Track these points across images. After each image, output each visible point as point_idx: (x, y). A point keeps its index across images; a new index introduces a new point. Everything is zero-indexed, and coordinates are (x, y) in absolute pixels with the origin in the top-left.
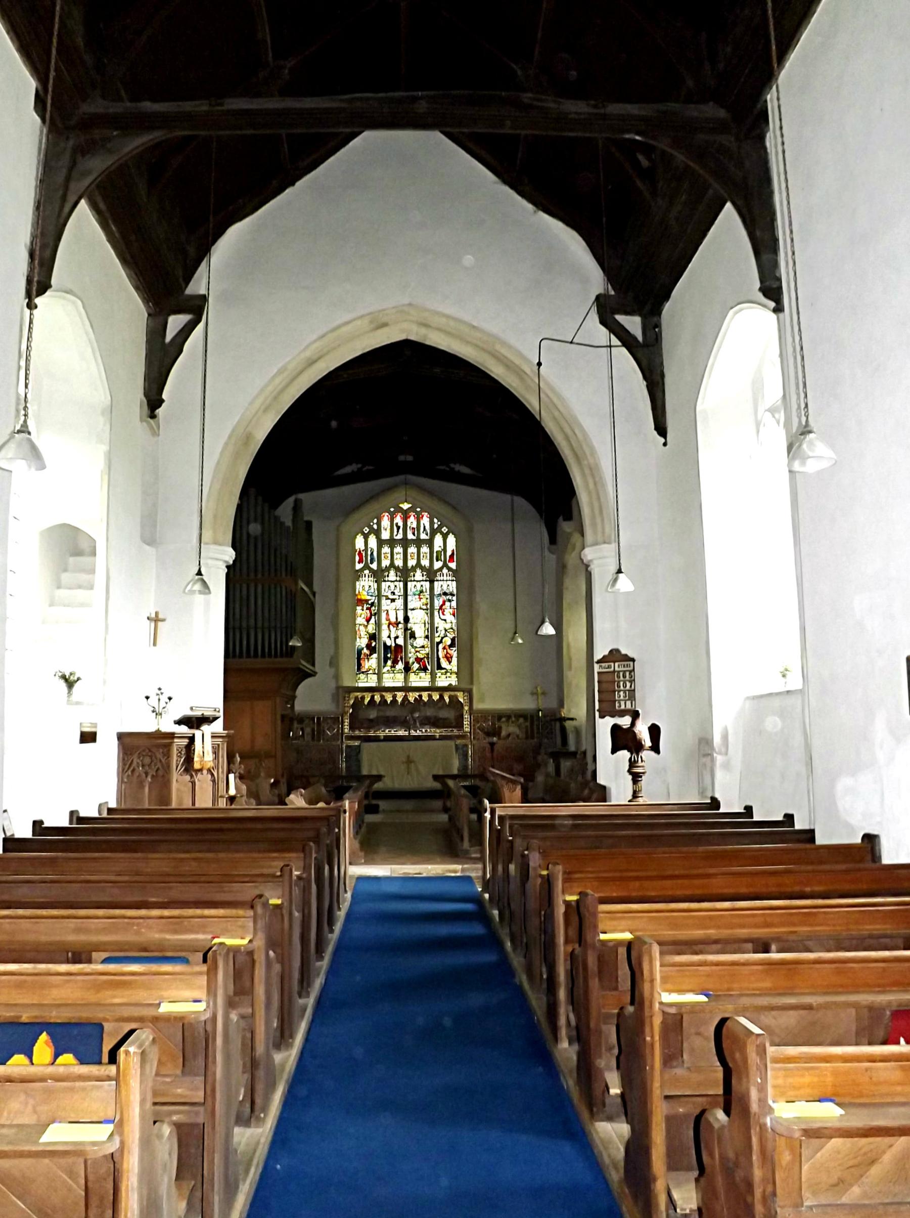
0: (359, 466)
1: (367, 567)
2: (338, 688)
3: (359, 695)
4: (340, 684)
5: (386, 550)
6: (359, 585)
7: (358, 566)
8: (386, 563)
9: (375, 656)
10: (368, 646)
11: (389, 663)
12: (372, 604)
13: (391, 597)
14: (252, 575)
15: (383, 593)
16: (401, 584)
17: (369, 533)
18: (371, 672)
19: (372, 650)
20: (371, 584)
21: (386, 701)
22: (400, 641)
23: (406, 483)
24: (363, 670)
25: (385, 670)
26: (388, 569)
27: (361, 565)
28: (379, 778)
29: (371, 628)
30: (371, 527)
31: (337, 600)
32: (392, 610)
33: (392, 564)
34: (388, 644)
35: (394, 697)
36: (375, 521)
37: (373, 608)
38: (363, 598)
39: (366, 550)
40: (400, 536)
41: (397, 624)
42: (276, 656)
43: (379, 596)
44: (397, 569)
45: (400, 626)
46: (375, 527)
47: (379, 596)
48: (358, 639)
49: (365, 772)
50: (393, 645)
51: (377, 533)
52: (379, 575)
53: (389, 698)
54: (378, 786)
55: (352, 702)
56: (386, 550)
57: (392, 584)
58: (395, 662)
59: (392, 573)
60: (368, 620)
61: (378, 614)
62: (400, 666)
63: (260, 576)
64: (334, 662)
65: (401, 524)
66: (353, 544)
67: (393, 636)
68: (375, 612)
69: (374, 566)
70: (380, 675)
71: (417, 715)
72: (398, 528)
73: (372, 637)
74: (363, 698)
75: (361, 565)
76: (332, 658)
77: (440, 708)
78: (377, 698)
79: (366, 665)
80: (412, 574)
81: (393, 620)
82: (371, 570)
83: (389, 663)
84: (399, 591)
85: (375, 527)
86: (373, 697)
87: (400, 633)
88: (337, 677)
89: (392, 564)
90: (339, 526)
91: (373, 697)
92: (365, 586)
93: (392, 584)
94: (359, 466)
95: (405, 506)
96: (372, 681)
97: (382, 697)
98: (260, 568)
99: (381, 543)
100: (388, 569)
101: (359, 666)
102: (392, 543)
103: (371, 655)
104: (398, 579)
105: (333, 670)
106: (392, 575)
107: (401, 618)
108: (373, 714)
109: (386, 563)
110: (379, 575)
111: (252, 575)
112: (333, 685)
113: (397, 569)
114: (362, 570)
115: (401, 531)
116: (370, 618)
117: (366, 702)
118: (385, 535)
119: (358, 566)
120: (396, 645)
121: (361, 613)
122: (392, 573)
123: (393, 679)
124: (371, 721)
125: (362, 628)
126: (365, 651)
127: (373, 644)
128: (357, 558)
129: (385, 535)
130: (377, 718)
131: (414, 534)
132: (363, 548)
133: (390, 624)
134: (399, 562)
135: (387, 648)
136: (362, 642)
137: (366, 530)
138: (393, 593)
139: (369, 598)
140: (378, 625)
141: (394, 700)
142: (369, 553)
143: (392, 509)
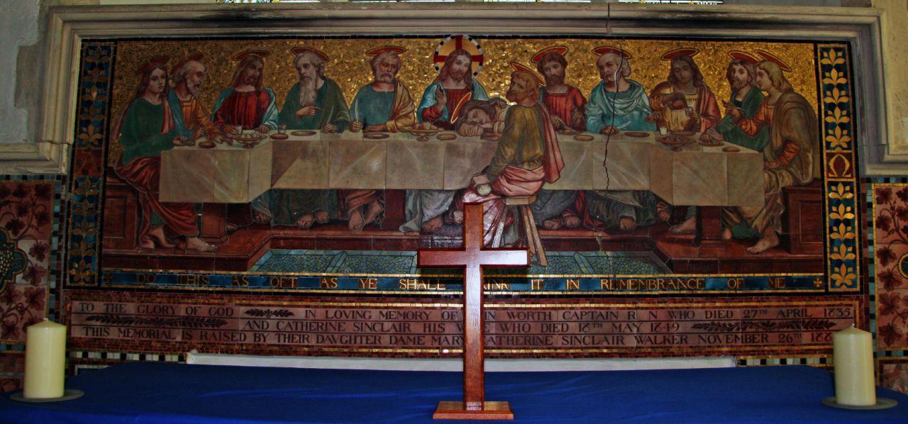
71: (522, 188)
77: (675, 143)
124: (238, 214)
130: (277, 197)
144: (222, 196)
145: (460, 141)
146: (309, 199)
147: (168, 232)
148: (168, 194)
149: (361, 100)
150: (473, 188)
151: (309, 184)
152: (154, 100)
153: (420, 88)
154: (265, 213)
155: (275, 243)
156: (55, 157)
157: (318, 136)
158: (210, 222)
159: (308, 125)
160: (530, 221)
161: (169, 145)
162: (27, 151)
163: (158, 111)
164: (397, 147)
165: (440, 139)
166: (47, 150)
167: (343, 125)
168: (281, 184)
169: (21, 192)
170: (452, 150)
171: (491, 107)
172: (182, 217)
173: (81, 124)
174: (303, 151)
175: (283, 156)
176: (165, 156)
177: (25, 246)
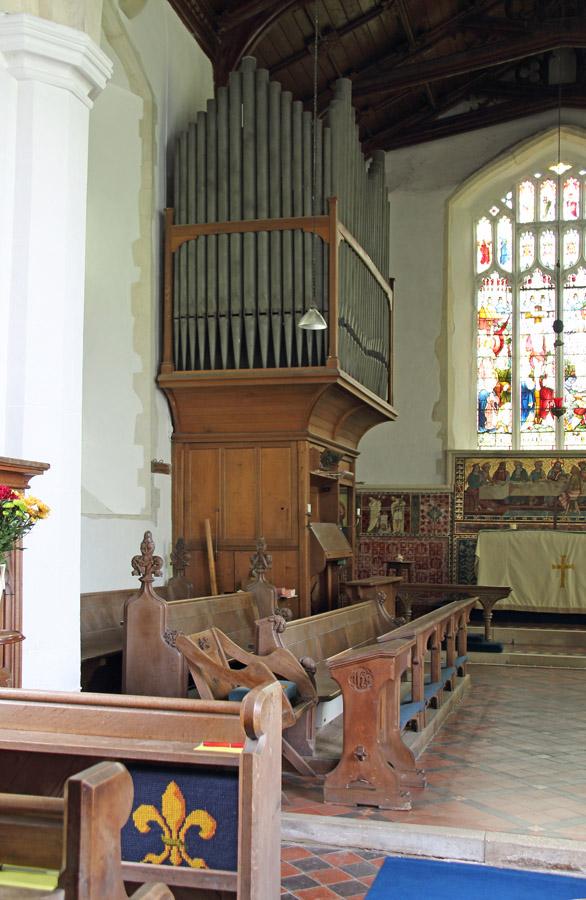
0: (481, 101)
1: (495, 267)
2: (445, 453)
3: (481, 462)
4: (450, 446)
5: (527, 240)
6: (482, 297)
7: (481, 268)
8: (526, 261)
9: (508, 406)
10: (497, 391)
11: (531, 416)
12: (504, 326)
13: (536, 313)
14: (250, 215)
15: (522, 308)
16: (553, 293)
17: (500, 215)
18: (501, 430)
19: (503, 395)
20: (503, 294)
21: (524, 472)
22: (550, 383)
23: (559, 123)
24: (488, 427)
25: (523, 427)
26: (530, 271)
27: (486, 266)
28: (505, 592)
29: (503, 363)
30: (502, 207)
31: (444, 319)
32: (536, 334)
33: (537, 264)
34: (530, 388)
35: (538, 465)
36: (509, 195)
37: (505, 332)
38: (489, 316)
39: (494, 242)
40: (551, 217)
41: (545, 356)
42: (295, 364)
43: (515, 313)
44: (545, 270)
45: (551, 359)
46: (509, 205)
47: (515, 313)
48: (480, 381)
49: (482, 582)
50: (538, 388)
51: (513, 214)
52: (515, 281)
53: (529, 469)
54: (504, 603)
55: (468, 473)
56: (527, 240)
57: (537, 297)
58: (541, 414)
59: (537, 276)
60: (497, 353)
61: (513, 341)
62: (549, 420)
63: (264, 215)
64: (440, 412)
65: (552, 198)
66: (473, 236)
67: (537, 374)
68: (507, 336)
69: (508, 267)
70: (515, 434)
72: (549, 204)
73: (506, 377)
74: (486, 468)
75: (486, 266)
76: (437, 404)
78: (510, 468)
79: (493, 419)
80: (570, 276)
81: (538, 350)
82: (502, 273)
83: (531, 416)
84: (549, 304)
85: (509, 205)
86: (502, 465)
87: (550, 370)
88: (444, 434)
89: (537, 264)
90: (447, 201)
91: (502, 465)
92: (493, 300)
93: (537, 297)
94: (481, 101)
95: (560, 168)
96: (503, 443)
97: (516, 464)
98: (264, 204)
99: (518, 229)
100: (530, 271)
101: (482, 421)
102: (537, 228)
103: (501, 403)
104: (547, 285)
105: (438, 425)
106: (537, 279)
107: (550, 348)
108: (501, 492)
109: (526, 261)
110: (515, 281)
111: (250, 215)
112: (439, 447)
113: (545, 270)
114: (487, 273)
115: (552, 208)
116: (501, 347)
117: (492, 473)
118: (526, 216)
119: (481, 268)
120: (543, 388)
121: (486, 341)
122: (537, 276)
123: (538, 437)
124: (500, 502)
125: (487, 363)
126: (493, 399)
127: (506, 386)
128: (480, 256)
129: (526, 216)
130: (511, 498)
131: (575, 213)
132: (489, 238)
133: (531, 357)
134: (548, 260)
135: (526, 392)
136: (486, 385)
137: (495, 211)
138: (539, 308)
139: (496, 316)
140: (513, 357)
141: (538, 474)
142: (499, 246)
143: (538, 176)
144: (496, 498)
145: (557, 484)
146: (519, 498)
147: (482, 505)
148: (481, 497)
149: (532, 474)
150: (561, 496)
151: (519, 494)
152: (476, 474)
153: (547, 469)
154: (507, 502)
155: (510, 509)
156: (450, 487)
157: (520, 483)
158: (493, 504)
159: (518, 480)
160: (576, 503)
161: (481, 485)
162: (444, 487)
163: (478, 476)
164: (542, 486)
165: (552, 484)
166: (449, 486)
167: (528, 480)
168: (513, 494)
169: (440, 497)
170: (557, 487)
171: (566, 476)
172: (484, 504)
173: (457, 480)
174: (517, 487)
175: (512, 487)
176: (481, 488)
177: (442, 510)
